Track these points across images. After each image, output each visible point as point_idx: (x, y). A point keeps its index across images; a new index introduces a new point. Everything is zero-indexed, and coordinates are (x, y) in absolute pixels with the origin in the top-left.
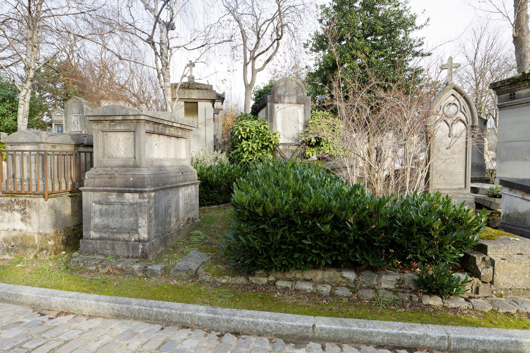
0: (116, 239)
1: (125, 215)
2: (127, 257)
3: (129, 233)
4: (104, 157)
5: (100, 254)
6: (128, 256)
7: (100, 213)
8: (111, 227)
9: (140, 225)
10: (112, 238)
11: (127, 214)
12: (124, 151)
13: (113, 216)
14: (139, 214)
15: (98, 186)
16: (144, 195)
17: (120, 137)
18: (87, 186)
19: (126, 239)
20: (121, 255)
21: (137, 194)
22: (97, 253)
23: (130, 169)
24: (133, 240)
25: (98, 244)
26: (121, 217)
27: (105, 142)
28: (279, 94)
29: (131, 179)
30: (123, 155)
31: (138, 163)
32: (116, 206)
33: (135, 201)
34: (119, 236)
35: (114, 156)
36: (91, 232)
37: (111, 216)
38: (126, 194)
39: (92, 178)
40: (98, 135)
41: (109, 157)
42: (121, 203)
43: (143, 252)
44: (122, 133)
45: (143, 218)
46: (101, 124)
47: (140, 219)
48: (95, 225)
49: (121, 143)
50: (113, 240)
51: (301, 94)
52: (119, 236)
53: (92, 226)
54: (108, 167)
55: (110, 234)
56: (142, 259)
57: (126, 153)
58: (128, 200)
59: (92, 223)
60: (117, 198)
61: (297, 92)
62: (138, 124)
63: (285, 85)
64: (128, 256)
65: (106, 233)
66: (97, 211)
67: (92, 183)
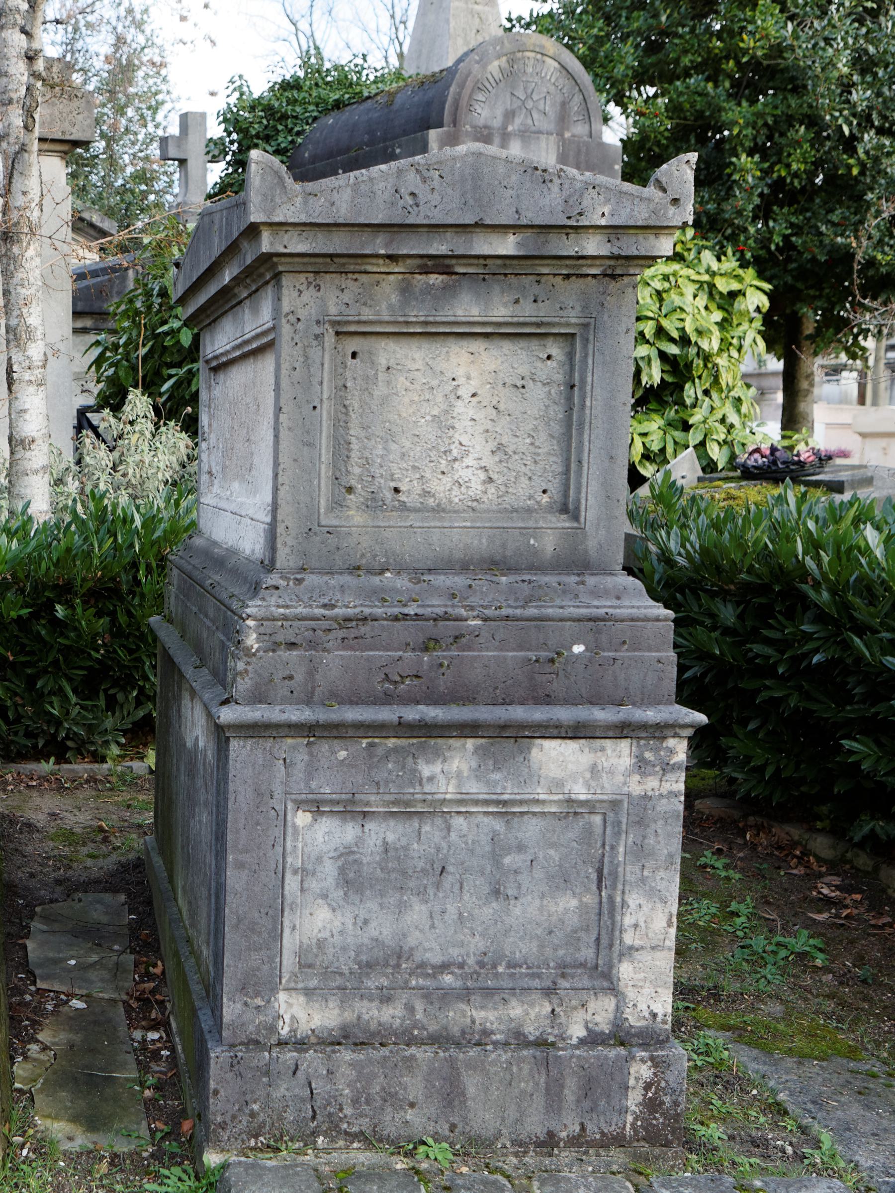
0: (456, 1031)
1: (524, 878)
2: (540, 1144)
3: (549, 992)
4: (337, 504)
5: (360, 1136)
6: (551, 1134)
7: (342, 871)
8: (418, 957)
9: (629, 938)
10: (433, 1028)
11: (538, 874)
12: (489, 461)
13: (438, 886)
14: (631, 872)
15: (337, 698)
16: (671, 751)
17: (460, 372)
18: (258, 697)
19: (531, 1031)
20: (498, 1136)
21: (624, 745)
22: (334, 1130)
23: (551, 579)
24: (577, 1031)
25: (344, 1074)
26: (496, 893)
27: (354, 403)
28: (481, 122)
29: (578, 649)
30: (476, 487)
31: (592, 544)
32: (459, 822)
33: (608, 787)
34: (479, 1015)
35: (409, 498)
36: (282, 996)
37: (421, 893)
38: (548, 744)
39: (292, 645)
40: (315, 353)
41: (373, 504)
42: (505, 803)
43: (652, 1105)
44: (478, 345)
45: (654, 894)
46: (346, 282)
47: (633, 900)
48: (302, 953)
49: (464, 410)
50: (439, 1040)
51: (580, 129)
52: (479, 1015)
53: (289, 961)
54: (382, 572)
55: (419, 1006)
56: (644, 1147)
57: (499, 479)
58: (559, 784)
59: (290, 942)
60: (478, 774)
61: (563, 119)
62: (613, 286)
63: (510, 75)
64: (551, 1134)
65: (386, 1000)
66: (319, 860)
67: (299, 677)
